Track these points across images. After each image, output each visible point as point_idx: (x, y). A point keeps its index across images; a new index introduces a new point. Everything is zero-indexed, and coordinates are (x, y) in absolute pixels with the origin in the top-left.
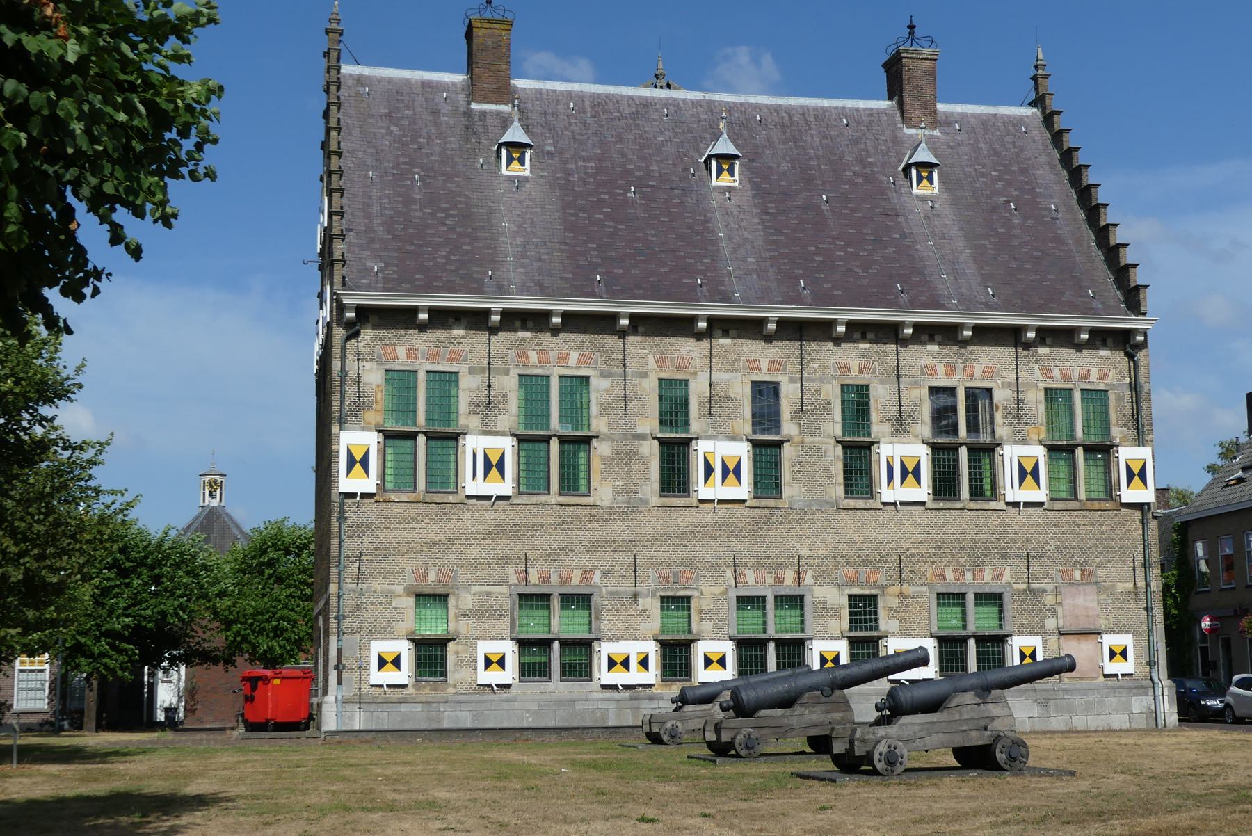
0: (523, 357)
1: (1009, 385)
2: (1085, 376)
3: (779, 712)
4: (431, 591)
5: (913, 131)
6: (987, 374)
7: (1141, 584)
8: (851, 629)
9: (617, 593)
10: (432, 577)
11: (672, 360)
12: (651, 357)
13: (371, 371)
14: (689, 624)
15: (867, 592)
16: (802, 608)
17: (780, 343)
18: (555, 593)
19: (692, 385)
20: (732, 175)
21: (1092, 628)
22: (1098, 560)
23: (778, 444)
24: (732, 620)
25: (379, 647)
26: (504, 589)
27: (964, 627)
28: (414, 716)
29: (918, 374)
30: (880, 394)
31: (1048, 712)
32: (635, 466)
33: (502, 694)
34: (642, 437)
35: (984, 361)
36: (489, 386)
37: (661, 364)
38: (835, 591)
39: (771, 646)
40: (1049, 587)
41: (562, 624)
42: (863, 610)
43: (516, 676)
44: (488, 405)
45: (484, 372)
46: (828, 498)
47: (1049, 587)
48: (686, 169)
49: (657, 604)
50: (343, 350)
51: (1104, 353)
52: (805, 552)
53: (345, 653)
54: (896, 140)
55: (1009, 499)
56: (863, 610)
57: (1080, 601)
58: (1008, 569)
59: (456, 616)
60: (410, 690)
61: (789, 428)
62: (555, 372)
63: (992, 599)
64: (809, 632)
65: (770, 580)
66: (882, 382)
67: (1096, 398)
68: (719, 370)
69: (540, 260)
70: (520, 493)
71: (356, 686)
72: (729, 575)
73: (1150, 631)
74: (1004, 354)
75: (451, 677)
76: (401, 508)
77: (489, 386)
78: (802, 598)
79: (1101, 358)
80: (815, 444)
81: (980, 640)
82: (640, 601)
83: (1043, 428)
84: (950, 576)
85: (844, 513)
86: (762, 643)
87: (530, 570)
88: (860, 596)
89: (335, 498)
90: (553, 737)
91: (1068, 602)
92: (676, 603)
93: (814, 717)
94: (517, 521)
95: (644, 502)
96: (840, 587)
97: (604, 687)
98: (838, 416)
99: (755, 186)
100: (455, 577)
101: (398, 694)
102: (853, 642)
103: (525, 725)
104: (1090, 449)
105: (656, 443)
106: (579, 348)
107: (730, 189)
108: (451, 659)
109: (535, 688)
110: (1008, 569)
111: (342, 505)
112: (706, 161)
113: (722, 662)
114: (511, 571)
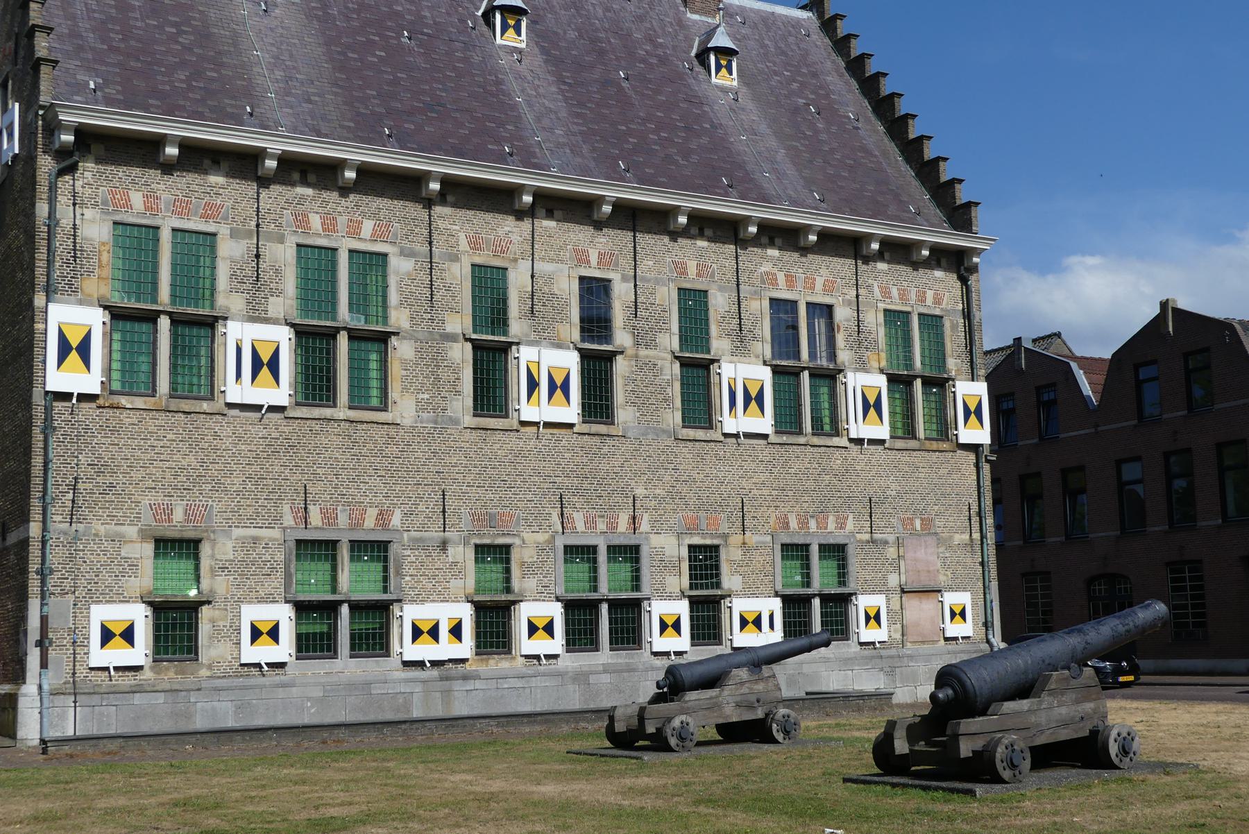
0: (302, 222)
1: (849, 303)
2: (922, 299)
3: (1024, 704)
4: (177, 535)
5: (696, 17)
6: (828, 289)
7: (976, 536)
8: (691, 588)
9: (421, 540)
10: (178, 515)
11: (488, 241)
12: (462, 236)
13: (93, 221)
14: (508, 580)
15: (708, 542)
16: (637, 560)
17: (611, 232)
18: (345, 538)
19: (511, 275)
20: (519, 33)
21: (932, 584)
22: (936, 508)
24: (558, 574)
25: (101, 614)
26: (276, 533)
27: (808, 585)
28: (153, 713)
29: (758, 283)
30: (719, 302)
31: (894, 682)
32: (444, 375)
33: (274, 677)
34: (452, 338)
35: (823, 271)
36: (258, 256)
37: (475, 245)
38: (674, 540)
39: (604, 608)
40: (891, 538)
41: (354, 580)
42: (704, 563)
43: (293, 651)
44: (256, 281)
45: (251, 238)
46: (664, 426)
47: (891, 538)
48: (463, 21)
49: (471, 554)
50: (53, 189)
51: (939, 274)
52: (640, 491)
53: (52, 623)
54: (681, 24)
55: (853, 435)
56: (704, 563)
57: (921, 554)
58: (851, 516)
59: (212, 570)
60: (147, 674)
61: (622, 338)
62: (345, 245)
63: (836, 552)
64: (646, 591)
65: (602, 526)
66: (721, 289)
67: (932, 323)
68: (543, 259)
69: (309, 101)
70: (298, 404)
71: (69, 669)
72: (555, 518)
73: (985, 588)
74: (843, 266)
75: (205, 654)
76: (135, 417)
77: (258, 256)
78: (636, 549)
79: (936, 279)
80: (647, 362)
81: (826, 599)
82: (451, 551)
83: (883, 355)
84: (794, 524)
85: (682, 444)
86: (593, 605)
87: (311, 507)
88: (700, 547)
89: (38, 398)
90: (371, 737)
91: (909, 555)
92: (494, 554)
93: (1064, 710)
94: (294, 441)
95: (455, 422)
96: (679, 535)
97: (406, 664)
98: (675, 327)
99: (544, 51)
100: (210, 518)
101: (128, 680)
102: (695, 603)
103: (307, 720)
104: (928, 382)
105: (469, 346)
106: (374, 216)
107: (520, 51)
108: (204, 629)
109: (318, 667)
110: (851, 516)
111: (48, 410)
112: (485, 15)
113: (549, 629)
114: (286, 508)
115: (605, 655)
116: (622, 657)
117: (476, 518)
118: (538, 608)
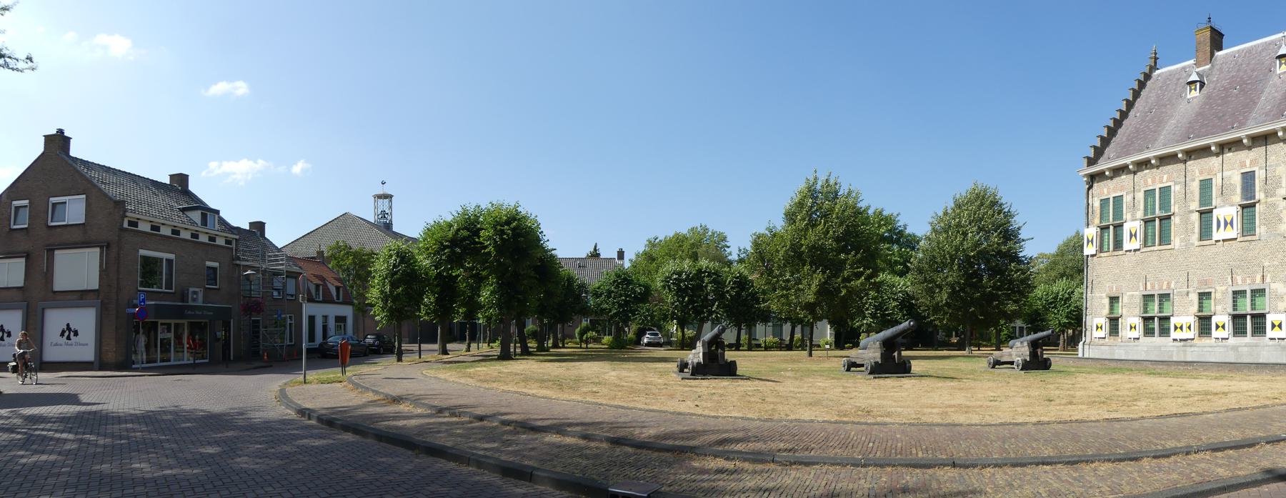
23: (1253, 205)
32: (1190, 227)
34: (1192, 212)
37: (1201, 173)
52: (1266, 264)
61: (1259, 195)
65: (1248, 281)
101: (1102, 341)
109: (1149, 339)
115: (1248, 339)
116: (1256, 340)
117: (1200, 282)
118: (1221, 317)
